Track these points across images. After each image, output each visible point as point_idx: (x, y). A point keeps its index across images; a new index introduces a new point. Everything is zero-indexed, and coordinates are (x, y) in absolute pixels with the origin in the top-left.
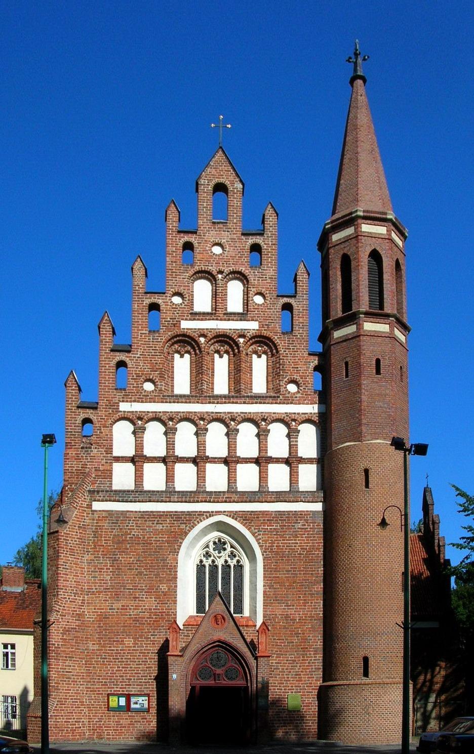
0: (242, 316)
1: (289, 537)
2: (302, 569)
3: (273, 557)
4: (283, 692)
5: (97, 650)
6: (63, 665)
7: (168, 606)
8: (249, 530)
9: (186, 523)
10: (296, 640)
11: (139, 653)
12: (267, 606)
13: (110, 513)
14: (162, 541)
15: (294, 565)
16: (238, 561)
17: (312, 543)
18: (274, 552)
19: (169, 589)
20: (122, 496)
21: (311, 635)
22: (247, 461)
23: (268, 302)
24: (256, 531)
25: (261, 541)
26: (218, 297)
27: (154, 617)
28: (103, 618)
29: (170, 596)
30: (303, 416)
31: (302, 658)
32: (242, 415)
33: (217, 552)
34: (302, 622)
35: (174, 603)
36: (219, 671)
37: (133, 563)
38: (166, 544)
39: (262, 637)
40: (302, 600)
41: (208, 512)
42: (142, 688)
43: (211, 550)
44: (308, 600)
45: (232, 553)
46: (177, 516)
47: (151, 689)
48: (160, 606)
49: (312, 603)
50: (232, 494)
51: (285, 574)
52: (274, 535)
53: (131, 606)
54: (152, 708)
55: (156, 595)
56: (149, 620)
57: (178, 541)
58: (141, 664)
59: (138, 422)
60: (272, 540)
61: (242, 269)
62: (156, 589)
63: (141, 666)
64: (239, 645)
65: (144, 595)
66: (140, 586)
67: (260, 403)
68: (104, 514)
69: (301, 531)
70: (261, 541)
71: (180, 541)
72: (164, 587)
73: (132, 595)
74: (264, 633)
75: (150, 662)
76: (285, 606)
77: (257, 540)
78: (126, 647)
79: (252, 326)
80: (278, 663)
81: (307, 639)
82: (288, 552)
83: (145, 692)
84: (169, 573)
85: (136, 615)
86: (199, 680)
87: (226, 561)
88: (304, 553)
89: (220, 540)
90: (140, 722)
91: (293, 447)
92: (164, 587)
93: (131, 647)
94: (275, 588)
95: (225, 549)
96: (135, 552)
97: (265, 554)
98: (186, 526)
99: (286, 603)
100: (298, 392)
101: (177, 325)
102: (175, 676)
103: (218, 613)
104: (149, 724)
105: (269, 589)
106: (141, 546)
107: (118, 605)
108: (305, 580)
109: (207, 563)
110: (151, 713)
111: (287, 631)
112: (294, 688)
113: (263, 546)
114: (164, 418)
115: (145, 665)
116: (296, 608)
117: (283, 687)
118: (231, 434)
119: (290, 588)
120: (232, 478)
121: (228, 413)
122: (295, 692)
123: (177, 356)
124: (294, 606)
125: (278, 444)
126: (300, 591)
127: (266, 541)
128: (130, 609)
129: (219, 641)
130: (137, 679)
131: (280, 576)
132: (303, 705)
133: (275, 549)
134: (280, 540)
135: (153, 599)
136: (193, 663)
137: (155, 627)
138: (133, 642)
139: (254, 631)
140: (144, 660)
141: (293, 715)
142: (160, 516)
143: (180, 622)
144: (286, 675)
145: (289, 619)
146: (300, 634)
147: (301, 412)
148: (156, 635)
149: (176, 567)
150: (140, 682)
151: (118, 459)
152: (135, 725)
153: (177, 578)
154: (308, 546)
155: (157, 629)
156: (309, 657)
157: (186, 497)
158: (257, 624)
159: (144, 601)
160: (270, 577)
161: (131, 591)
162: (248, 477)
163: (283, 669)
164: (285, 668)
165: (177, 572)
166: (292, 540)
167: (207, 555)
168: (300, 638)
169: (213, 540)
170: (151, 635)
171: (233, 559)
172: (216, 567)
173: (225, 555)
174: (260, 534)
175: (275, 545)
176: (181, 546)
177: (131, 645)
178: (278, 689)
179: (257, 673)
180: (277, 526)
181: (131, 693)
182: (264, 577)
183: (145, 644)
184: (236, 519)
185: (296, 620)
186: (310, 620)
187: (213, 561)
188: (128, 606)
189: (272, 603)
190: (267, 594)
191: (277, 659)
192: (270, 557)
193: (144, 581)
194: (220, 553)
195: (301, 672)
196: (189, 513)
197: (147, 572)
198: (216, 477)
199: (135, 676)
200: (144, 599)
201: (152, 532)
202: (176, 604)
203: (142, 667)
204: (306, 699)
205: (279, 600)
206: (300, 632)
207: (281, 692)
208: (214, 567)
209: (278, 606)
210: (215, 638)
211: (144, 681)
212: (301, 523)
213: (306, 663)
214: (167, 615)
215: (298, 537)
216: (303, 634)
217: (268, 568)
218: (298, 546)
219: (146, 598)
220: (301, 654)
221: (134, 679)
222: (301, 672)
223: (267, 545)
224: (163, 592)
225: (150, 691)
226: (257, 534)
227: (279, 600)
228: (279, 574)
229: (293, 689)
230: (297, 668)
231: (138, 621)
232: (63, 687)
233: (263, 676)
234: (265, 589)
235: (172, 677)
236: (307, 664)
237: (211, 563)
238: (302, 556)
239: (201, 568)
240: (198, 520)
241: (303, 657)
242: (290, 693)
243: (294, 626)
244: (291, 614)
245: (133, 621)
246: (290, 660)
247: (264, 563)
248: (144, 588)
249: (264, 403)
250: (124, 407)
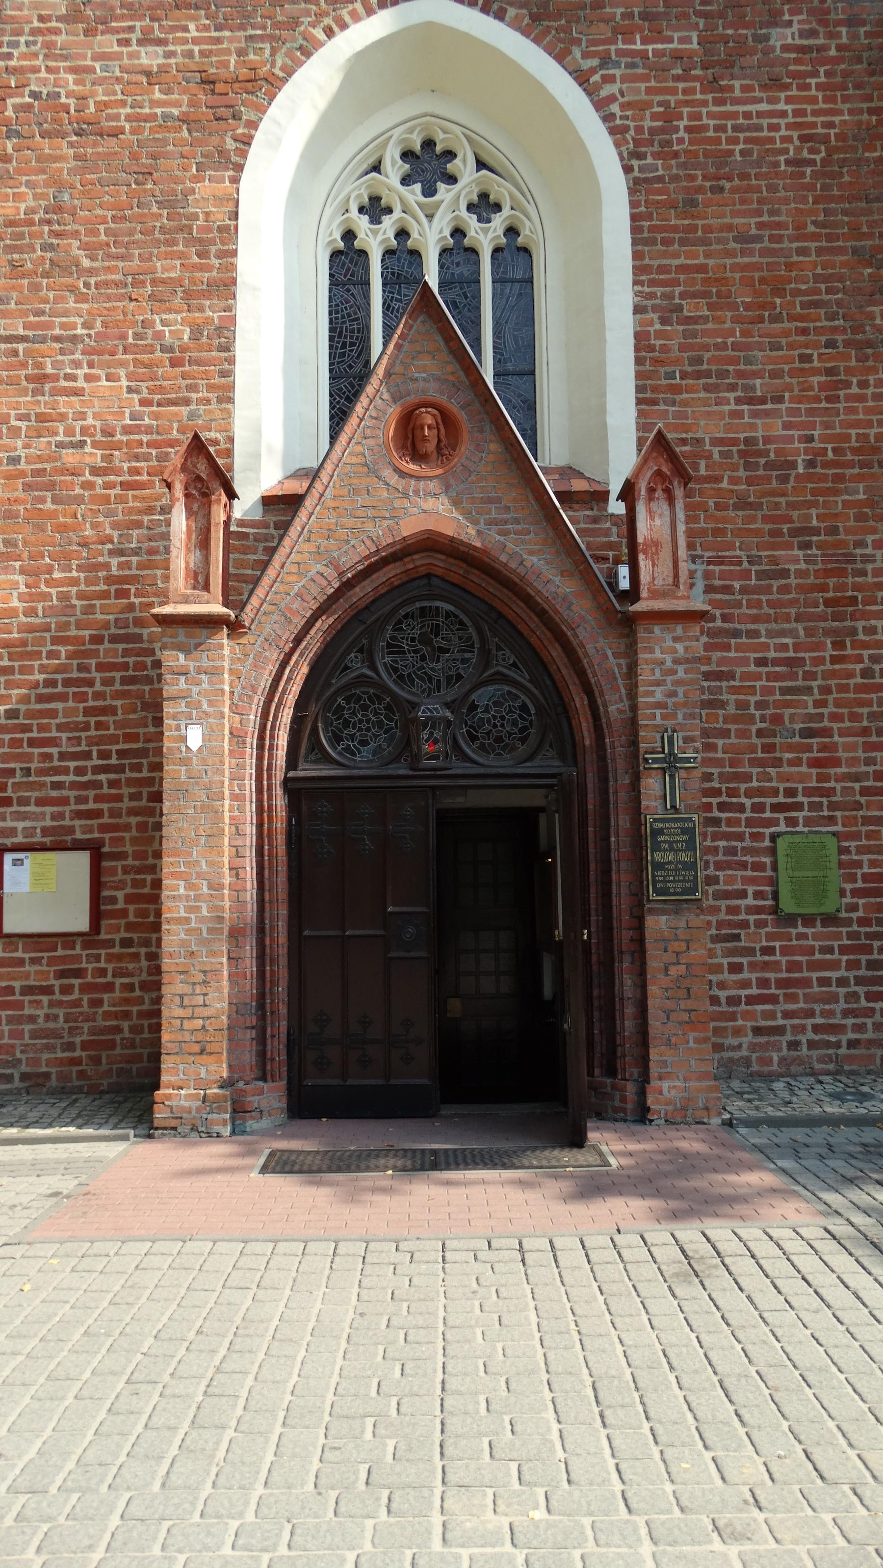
1: (744, 89)
2: (811, 228)
3: (675, 178)
4: (749, 823)
7: (192, 416)
8: (560, 58)
9: (271, 38)
10: (794, 559)
11: (55, 641)
12: (654, 402)
14: (165, 116)
15: (771, 213)
16: (512, 231)
17: (851, 112)
18: (676, 155)
19: (196, 332)
21: (870, 539)
24: (595, 62)
25: (615, 108)
27: (126, 466)
31: (829, 652)
33: (418, 187)
34: (823, 478)
35: (220, 400)
37: (30, 223)
38: (185, 133)
39: (651, 514)
40: (816, 372)
42: (61, 816)
44: (849, 371)
45: (484, 196)
47: (106, 820)
48: (156, 416)
49: (863, 384)
51: (731, 254)
52: (677, 78)
53: (19, 418)
54: (113, 914)
55: (137, 363)
56: (99, 481)
57: (236, 117)
58: (63, 697)
60: (665, 104)
62: (137, 336)
63: (59, 706)
64: (535, 559)
65: (77, 364)
66: (63, 326)
69: (797, 61)
70: (615, 108)
72: (174, 327)
73: (24, 365)
74: (659, 493)
75: (106, 682)
76: (738, 401)
77: (599, 105)
80: (718, 676)
81: (850, 558)
82: (742, 152)
83: (79, 835)
84: (195, 259)
85: (40, 459)
86: (327, 759)
88: (818, 158)
89: (429, 144)
90: (47, 990)
92: (174, 327)
94: (688, 320)
96: (43, 172)
97: (635, 163)
98: (273, 53)
99: (745, 388)
102: (195, 737)
103: (412, 399)
104: (96, 1003)
105: (664, 321)
106: (71, 145)
108: (825, 279)
109: (375, 240)
110: (110, 943)
111: (753, 519)
112: (800, 799)
113: (626, 129)
115: (81, 697)
116: (792, 412)
117: (749, 794)
119: (761, 320)
122: (808, 822)
124: (779, 399)
126: (804, 331)
127: (641, 107)
128: (15, 432)
129: (430, 543)
130: (41, 772)
131: (711, 262)
132: (848, 887)
133: (681, 141)
134: (705, 103)
135: (124, 383)
137: (130, 511)
138: (23, 589)
139: (595, 520)
140: (75, 675)
141: (804, 936)
144: (760, 733)
145: (762, 461)
146: (816, 532)
148: (136, 552)
149: (229, 232)
150: (57, 786)
152: (27, 1011)
153: (234, 282)
154: (831, 125)
155: (139, 525)
156: (865, 645)
158: (611, 488)
159: (77, 392)
160: (662, 269)
161: (21, 347)
163: (742, 705)
164: (753, 699)
165: (234, 253)
166: (760, 101)
167: (375, 209)
168: (815, 551)
169: (397, 132)
170: (111, 553)
171: (489, 221)
172: (416, 255)
174: (608, 79)
175: (682, 124)
176: (252, 137)
177: (15, 603)
178: (722, 807)
179: (634, 708)
180: (688, 40)
181: (8, 842)
182: (638, 270)
183: (81, 596)
184: (500, 16)
185: (793, 465)
186: (863, 465)
187: (402, 234)
189: (676, 389)
190: (652, 349)
191: (717, 655)
192: (660, 179)
193: (82, 298)
194: (429, 191)
195: (834, 717)
197: (93, 259)
199: (29, 758)
200: (81, 383)
201: (118, 80)
202: (231, 400)
203: (67, 712)
204: (865, 858)
205: (708, 374)
206: (815, 523)
207: (737, 822)
208: (403, 257)
209: (706, 403)
210: (409, 527)
211: (72, 778)
212: (796, 27)
213: (851, 675)
215: (787, 87)
216: (834, 531)
217: (651, 229)
218: (789, 126)
219: (88, 378)
220: (827, 632)
221: (27, 772)
222: (834, 717)
223: (647, 123)
224: (171, 350)
225: (103, 828)
226: (596, 78)
227: (708, 374)
228: (707, 255)
229: (799, 807)
230: (809, 700)
231: (51, 486)
233: (669, 723)
234: (641, 323)
235: (184, 739)
236: (859, 680)
237: (391, 234)
238: (809, 170)
239: (347, 262)
240: (328, 21)
241: (838, 645)
242: (782, 828)
243: (784, 495)
244: (767, 440)
245: (28, 487)
246: (776, 662)
247: (633, 204)
248: (80, 331)
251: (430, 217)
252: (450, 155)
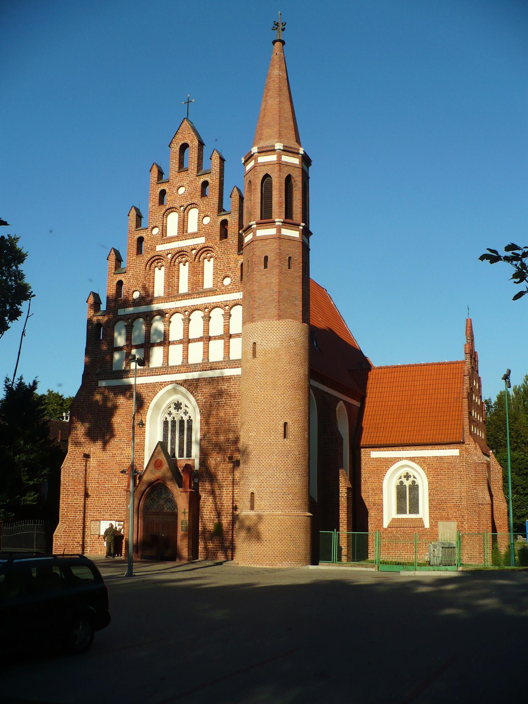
0: (194, 235)
5: (97, 487)
6: (72, 499)
23: (212, 222)
26: (183, 224)
30: (233, 302)
32: (192, 307)
41: (166, 382)
61: (195, 201)
67: (204, 296)
71: (148, 404)
78: (114, 484)
79: (201, 241)
91: (227, 327)
93: (116, 484)
95: (181, 408)
100: (230, 284)
101: (153, 249)
109: (170, 419)
120: (186, 357)
121: (183, 307)
125: (216, 327)
128: (117, 456)
147: (231, 299)
162: (196, 353)
167: (170, 414)
173: (181, 412)
174: (198, 396)
187: (174, 418)
188: (115, 454)
194: (178, 411)
214: (138, 460)
239: (166, 423)
249: (207, 296)
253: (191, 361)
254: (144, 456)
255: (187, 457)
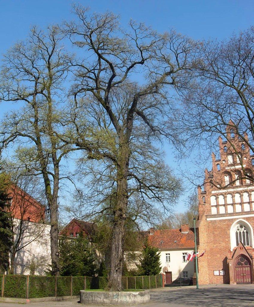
8: (248, 222)
13: (211, 221)
20: (214, 216)
22: (246, 203)
28: (211, 249)
29: (229, 242)
36: (242, 263)
43: (239, 228)
46: (229, 220)
50: (243, 213)
59: (217, 196)
68: (210, 221)
72: (227, 240)
77: (251, 225)
87: (243, 231)
92: (227, 240)
95: (243, 228)
101: (224, 168)
102: (230, 265)
107: (215, 246)
109: (238, 232)
114: (224, 194)
118: (241, 196)
120: (242, 209)
123: (225, 177)
129: (242, 254)
136: (236, 261)
142: (224, 221)
143: (232, 250)
149: (230, 234)
151: (212, 206)
157: (231, 215)
167: (238, 230)
187: (240, 231)
196: (232, 219)
198: (238, 208)
208: (240, 233)
210: (241, 254)
232: (202, 269)
239: (237, 233)
250: (213, 192)
251: (241, 230)
252: (242, 226)
253: (245, 210)
254: (230, 246)
255: (247, 245)
